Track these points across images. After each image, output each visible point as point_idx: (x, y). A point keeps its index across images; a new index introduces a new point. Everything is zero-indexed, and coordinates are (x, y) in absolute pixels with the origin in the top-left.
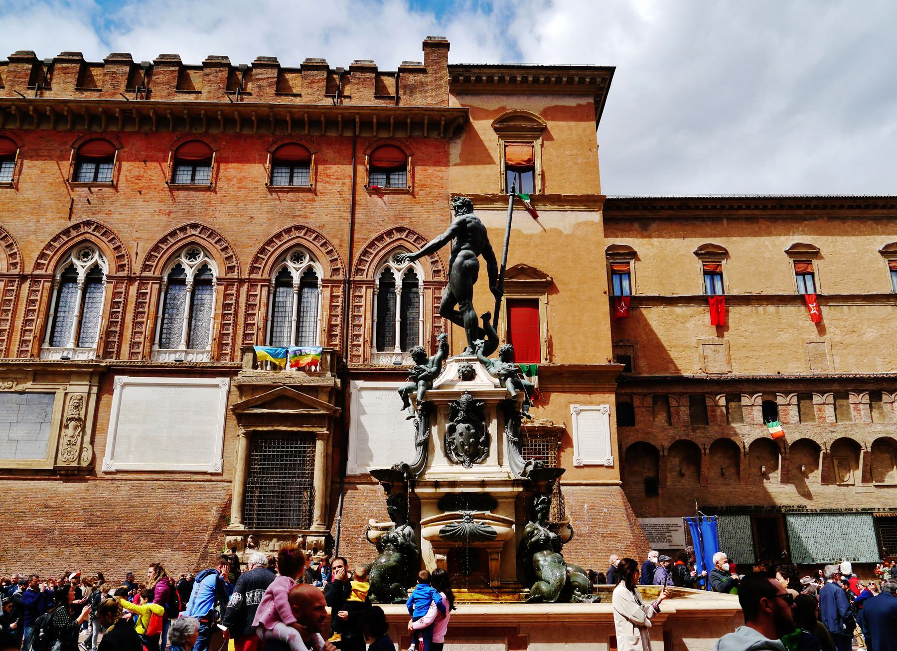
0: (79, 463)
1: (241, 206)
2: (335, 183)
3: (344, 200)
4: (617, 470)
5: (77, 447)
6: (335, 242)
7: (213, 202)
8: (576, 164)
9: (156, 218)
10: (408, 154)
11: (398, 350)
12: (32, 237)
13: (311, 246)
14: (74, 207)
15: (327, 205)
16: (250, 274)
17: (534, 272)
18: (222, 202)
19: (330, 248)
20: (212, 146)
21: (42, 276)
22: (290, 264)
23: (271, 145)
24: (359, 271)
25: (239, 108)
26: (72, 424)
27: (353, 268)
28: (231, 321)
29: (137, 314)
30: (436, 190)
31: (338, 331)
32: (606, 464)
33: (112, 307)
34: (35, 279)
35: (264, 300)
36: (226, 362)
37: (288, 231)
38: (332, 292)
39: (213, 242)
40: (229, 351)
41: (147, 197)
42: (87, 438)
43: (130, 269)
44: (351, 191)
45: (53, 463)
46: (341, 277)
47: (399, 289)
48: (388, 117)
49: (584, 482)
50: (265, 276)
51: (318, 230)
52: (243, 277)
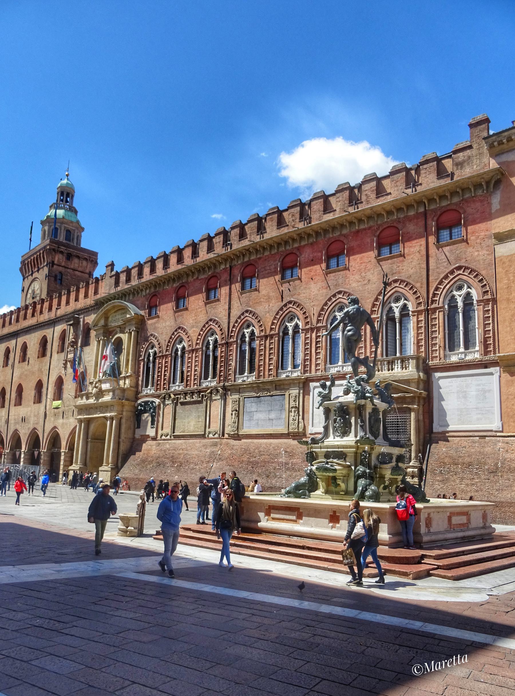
0: (298, 430)
1: (363, 274)
2: (415, 246)
3: (422, 256)
5: (297, 422)
6: (418, 285)
7: (348, 276)
9: (321, 292)
11: (462, 350)
12: (268, 314)
15: (412, 262)
18: (353, 275)
19: (415, 290)
20: (344, 241)
21: (274, 335)
23: (376, 231)
24: (433, 302)
25: (355, 215)
26: (293, 409)
27: (430, 300)
29: (317, 348)
30: (483, 234)
31: (423, 343)
33: (305, 346)
34: (272, 337)
38: (418, 318)
41: (316, 280)
42: (301, 417)
44: (425, 249)
46: (422, 308)
47: (460, 309)
51: (407, 280)
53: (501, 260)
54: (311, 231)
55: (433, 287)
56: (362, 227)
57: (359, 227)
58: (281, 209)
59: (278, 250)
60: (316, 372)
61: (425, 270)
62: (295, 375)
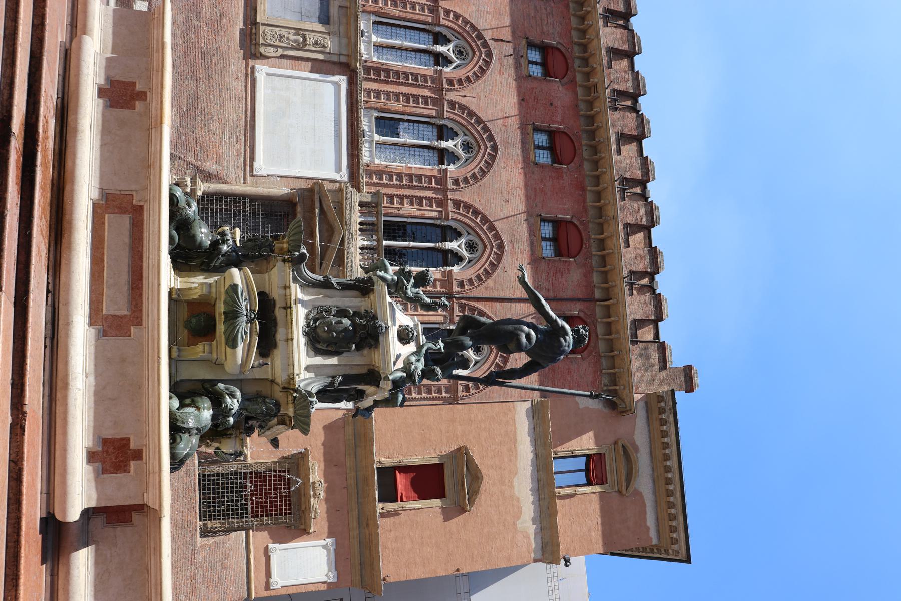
2: (547, 281)
4: (266, 594)
5: (277, 43)
6: (490, 283)
8: (589, 530)
10: (583, 354)
13: (484, 259)
14: (504, 43)
16: (453, 200)
17: (474, 493)
20: (572, 164)
21: (439, 15)
22: (463, 241)
23: (578, 220)
25: (610, 188)
27: (466, 302)
28: (405, 183)
29: (407, 96)
32: (271, 581)
33: (413, 74)
35: (427, 214)
36: (364, 179)
37: (497, 237)
39: (481, 165)
40: (375, 181)
43: (449, 90)
45: (263, 22)
46: (456, 289)
48: (618, 332)
49: (252, 557)
50: (451, 215)
51: (501, 266)
52: (449, 194)
53: (510, 410)
54: (598, 110)
55: (485, 306)
56: (589, 197)
57: (590, 191)
58: (636, 58)
59: (576, 43)
60: (365, 90)
61: (511, 296)
62: (363, 48)
